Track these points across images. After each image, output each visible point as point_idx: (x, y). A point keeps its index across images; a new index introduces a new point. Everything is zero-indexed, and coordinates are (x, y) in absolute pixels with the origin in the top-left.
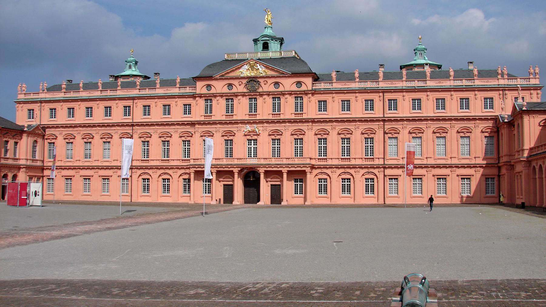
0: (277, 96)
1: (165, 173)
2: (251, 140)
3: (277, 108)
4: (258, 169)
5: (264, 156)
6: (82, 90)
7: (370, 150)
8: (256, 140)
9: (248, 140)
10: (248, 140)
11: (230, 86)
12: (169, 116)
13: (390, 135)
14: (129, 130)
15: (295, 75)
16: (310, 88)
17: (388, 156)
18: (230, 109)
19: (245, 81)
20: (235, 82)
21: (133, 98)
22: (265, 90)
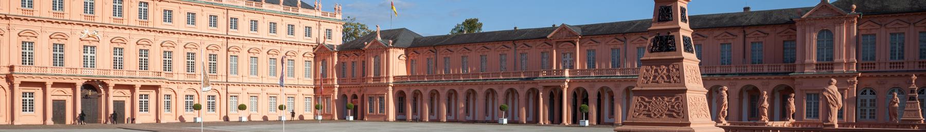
4: (107, 82)
5: (103, 67)
13: (231, 53)
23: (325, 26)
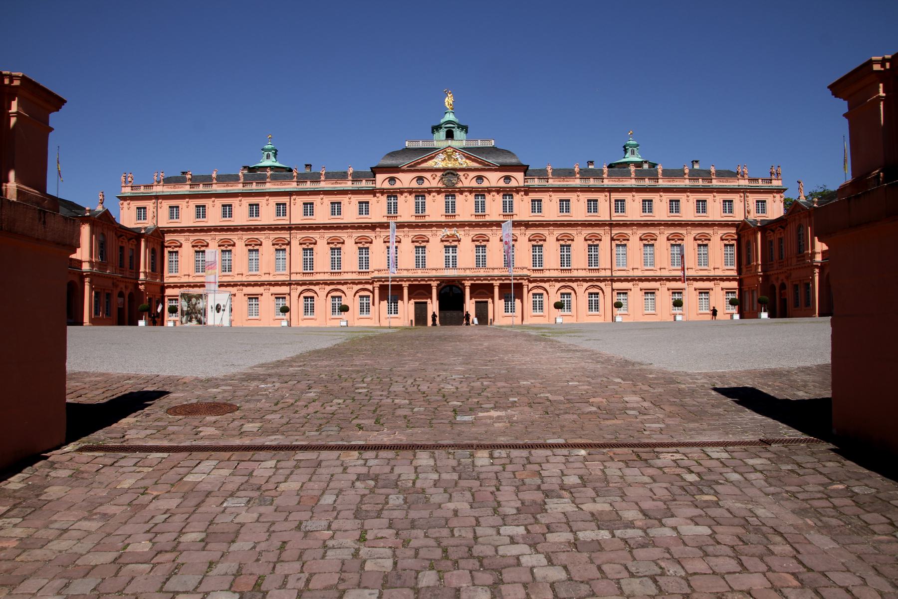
0: (480, 193)
1: (538, 287)
2: (449, 247)
3: (480, 207)
6: (215, 181)
7: (593, 259)
8: (456, 247)
9: (445, 247)
10: (445, 247)
11: (420, 179)
12: (595, 214)
14: (285, 235)
15: (503, 168)
16: (522, 184)
17: (615, 267)
18: (420, 208)
19: (439, 174)
20: (428, 175)
21: (289, 194)
22: (465, 185)
23: (752, 198)
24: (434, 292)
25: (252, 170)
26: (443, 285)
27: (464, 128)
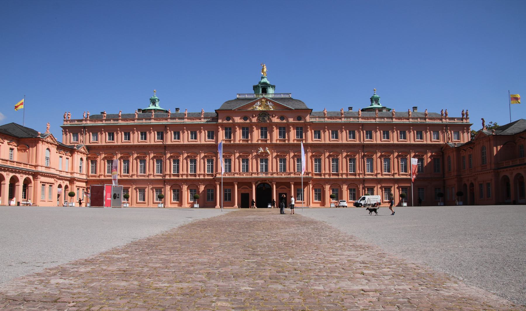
24: (254, 187)
25: (144, 111)
26: (259, 182)
27: (273, 87)
